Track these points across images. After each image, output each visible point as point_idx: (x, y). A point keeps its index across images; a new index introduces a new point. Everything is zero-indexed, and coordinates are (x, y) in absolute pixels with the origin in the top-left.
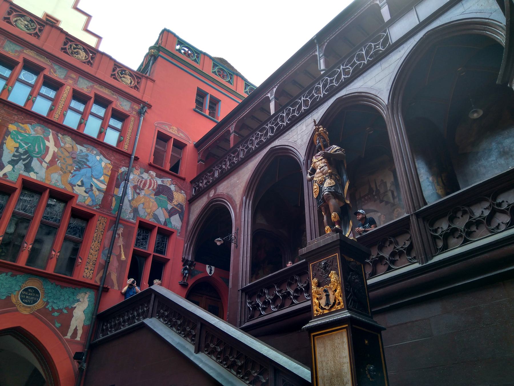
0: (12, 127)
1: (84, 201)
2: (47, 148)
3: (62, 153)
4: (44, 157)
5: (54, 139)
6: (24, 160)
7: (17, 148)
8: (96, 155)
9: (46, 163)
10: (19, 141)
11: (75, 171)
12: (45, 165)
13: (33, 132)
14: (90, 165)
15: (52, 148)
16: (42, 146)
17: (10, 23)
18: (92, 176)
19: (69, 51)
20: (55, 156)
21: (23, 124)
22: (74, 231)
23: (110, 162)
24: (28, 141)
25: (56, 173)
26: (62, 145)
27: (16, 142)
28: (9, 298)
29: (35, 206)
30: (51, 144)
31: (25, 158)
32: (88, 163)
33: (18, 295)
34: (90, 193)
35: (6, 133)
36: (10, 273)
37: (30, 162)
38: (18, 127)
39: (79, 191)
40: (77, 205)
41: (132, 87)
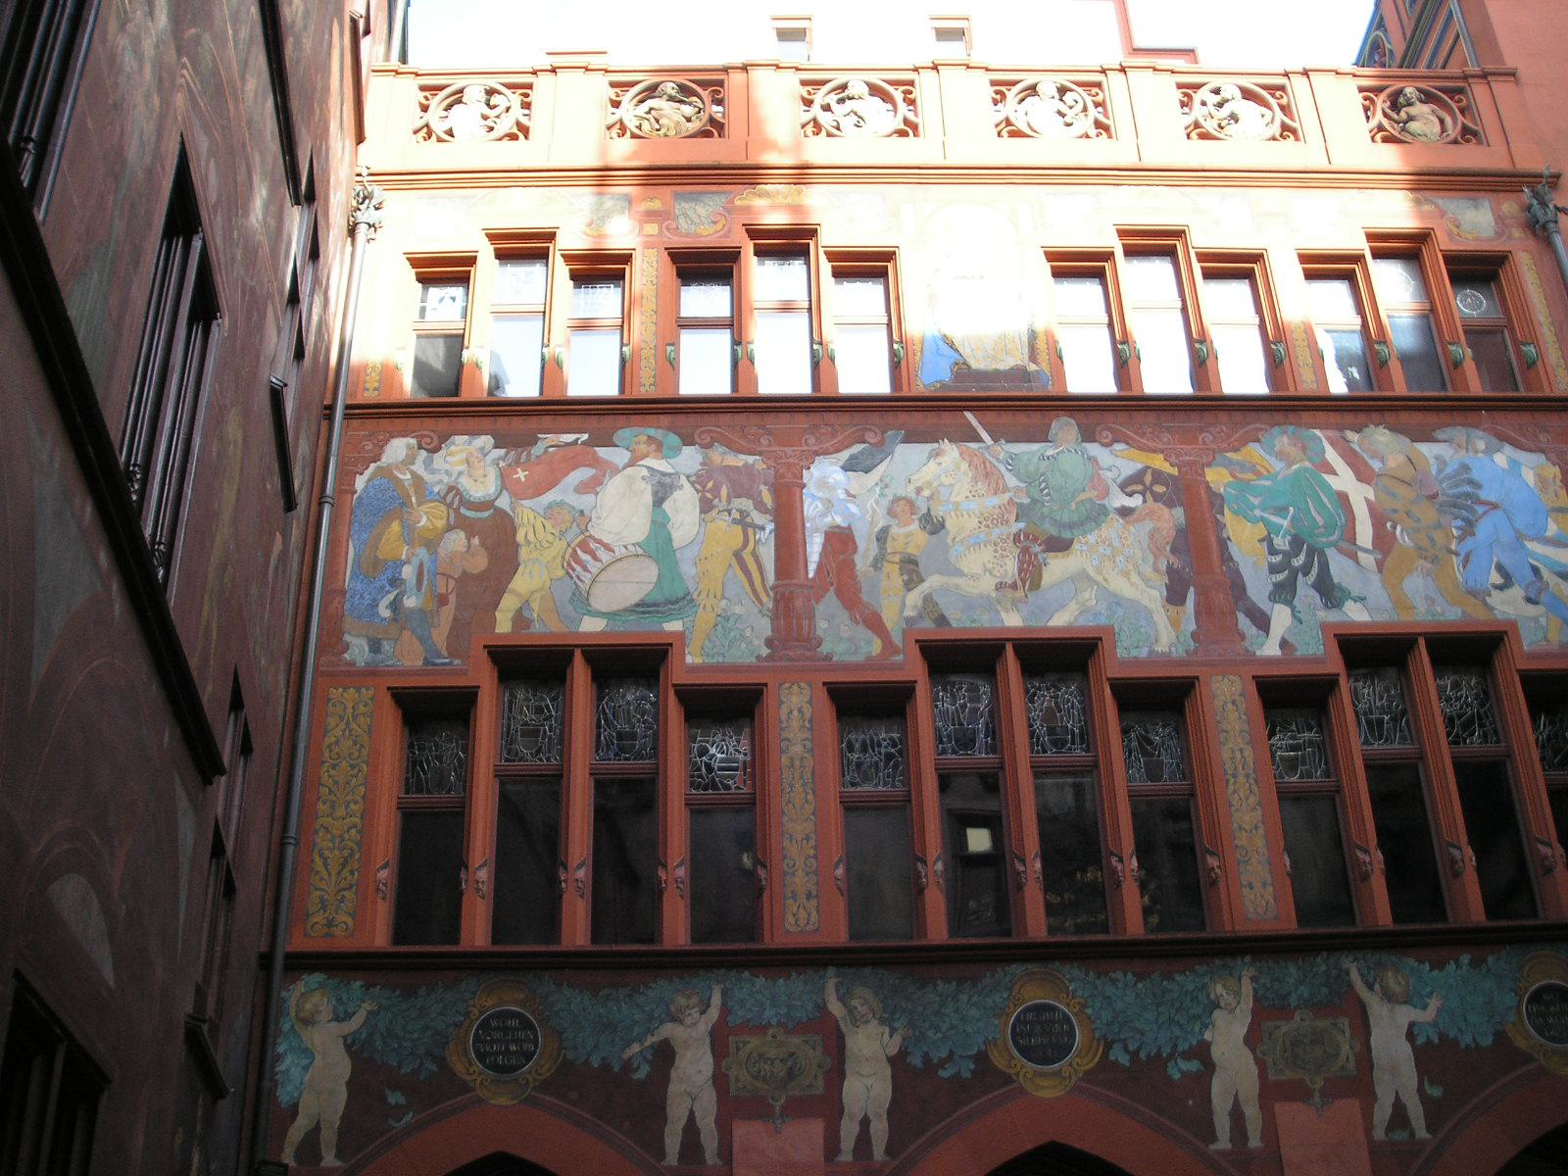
0: (1217, 477)
1: (1540, 635)
2: (1343, 499)
3: (1393, 495)
4: (1350, 535)
5: (1343, 457)
6: (1306, 570)
7: (1268, 540)
8: (1490, 451)
9: (1366, 551)
10: (1257, 513)
11: (1461, 539)
12: (1368, 560)
13: (1278, 466)
14: (1492, 498)
15: (1360, 496)
16: (1325, 500)
17: (1016, 134)
18: (1520, 537)
19: (1210, 126)
20: (1378, 518)
21: (1236, 450)
22: (1556, 752)
23: (1541, 458)
24: (1281, 502)
25: (1410, 571)
26: (1376, 465)
27: (1255, 521)
28: (1500, 1036)
29: (1404, 713)
30: (1344, 480)
31: (1304, 564)
32: (1483, 495)
33: (1521, 1020)
34: (1543, 597)
35: (1212, 505)
36: (1465, 959)
37: (1324, 567)
38: (1229, 465)
39: (1508, 606)
40: (1532, 656)
41: (1455, 142)
